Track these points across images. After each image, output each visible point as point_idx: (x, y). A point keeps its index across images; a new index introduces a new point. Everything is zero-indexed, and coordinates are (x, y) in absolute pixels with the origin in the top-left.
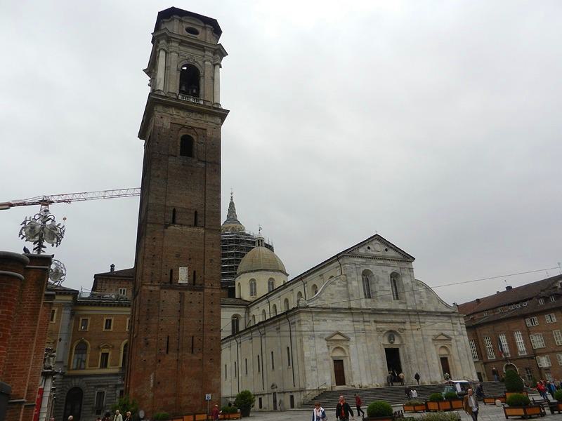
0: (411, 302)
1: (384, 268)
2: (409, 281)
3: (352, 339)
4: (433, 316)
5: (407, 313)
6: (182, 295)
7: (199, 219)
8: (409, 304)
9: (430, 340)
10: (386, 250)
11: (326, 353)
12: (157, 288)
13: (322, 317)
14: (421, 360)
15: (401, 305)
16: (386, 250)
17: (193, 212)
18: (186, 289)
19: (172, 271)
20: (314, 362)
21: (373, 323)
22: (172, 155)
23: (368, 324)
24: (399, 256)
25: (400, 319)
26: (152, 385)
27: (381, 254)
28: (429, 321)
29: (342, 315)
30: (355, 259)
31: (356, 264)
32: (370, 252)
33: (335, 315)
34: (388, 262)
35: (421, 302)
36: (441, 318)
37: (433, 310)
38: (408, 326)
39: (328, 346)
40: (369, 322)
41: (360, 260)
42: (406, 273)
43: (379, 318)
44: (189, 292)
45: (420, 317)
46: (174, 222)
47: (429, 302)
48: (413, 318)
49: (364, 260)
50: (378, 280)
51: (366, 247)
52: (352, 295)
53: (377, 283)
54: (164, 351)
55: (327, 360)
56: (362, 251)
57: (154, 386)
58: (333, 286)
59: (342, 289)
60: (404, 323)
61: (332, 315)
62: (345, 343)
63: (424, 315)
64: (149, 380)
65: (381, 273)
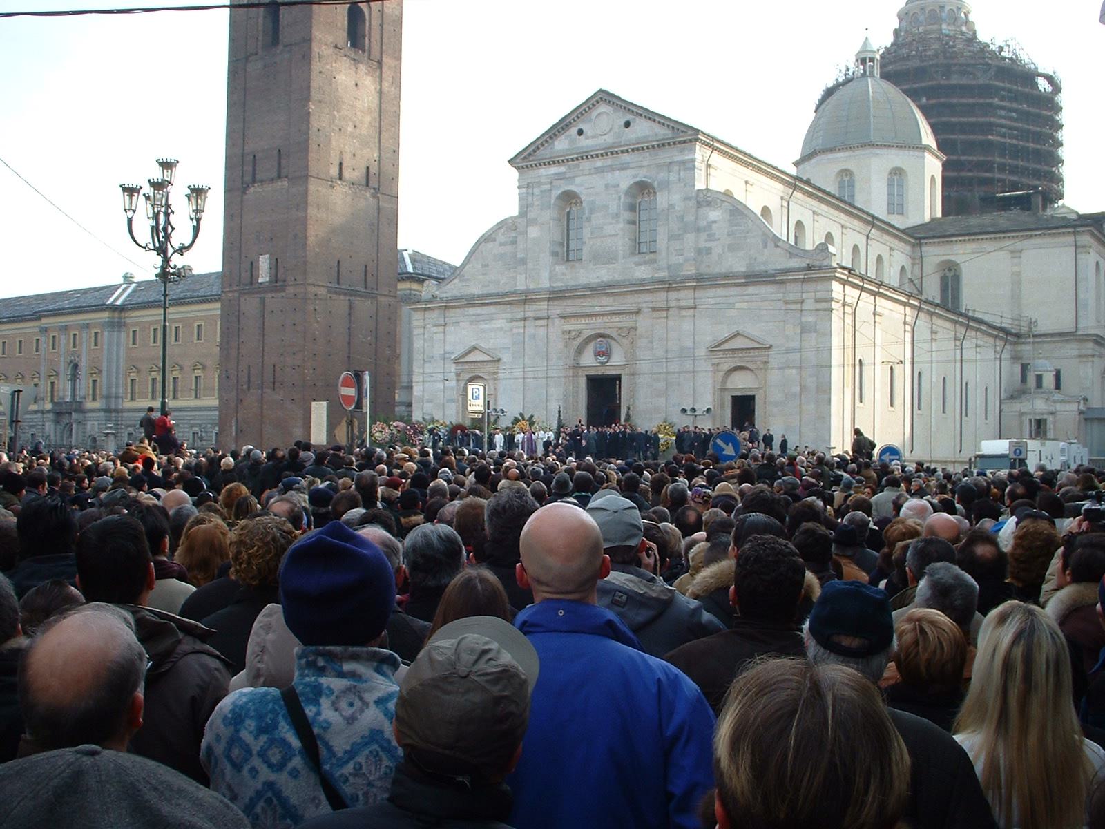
0: (676, 255)
1: (610, 177)
2: (676, 198)
3: (506, 357)
4: (724, 286)
5: (643, 287)
6: (263, 301)
7: (283, 162)
8: (663, 263)
9: (702, 352)
10: (627, 124)
11: (452, 388)
12: (236, 294)
13: (453, 314)
14: (662, 400)
15: (643, 268)
16: (627, 124)
17: (276, 152)
18: (266, 292)
19: (252, 263)
20: (431, 405)
21: (558, 322)
22: (252, 54)
23: (544, 322)
24: (662, 132)
25: (629, 302)
26: (234, 434)
27: (609, 139)
28: (710, 297)
29: (492, 309)
30: (544, 171)
31: (539, 184)
32: (584, 143)
33: (478, 310)
34: (626, 158)
35: (708, 251)
36: (750, 290)
37: (743, 269)
38: (643, 322)
39: (458, 375)
40: (548, 318)
41: (553, 170)
42: (673, 177)
43: (571, 307)
44: (269, 295)
45: (683, 294)
46: (254, 181)
47: (732, 248)
48: (660, 298)
49: (562, 169)
50: (592, 211)
51: (574, 131)
52: (523, 261)
53: (589, 220)
54: (245, 387)
55: (452, 401)
56: (561, 144)
57: (236, 434)
58: (490, 245)
59: (509, 249)
60: (637, 312)
61: (472, 311)
62: (489, 368)
63: (695, 288)
64: (231, 426)
65: (603, 189)
